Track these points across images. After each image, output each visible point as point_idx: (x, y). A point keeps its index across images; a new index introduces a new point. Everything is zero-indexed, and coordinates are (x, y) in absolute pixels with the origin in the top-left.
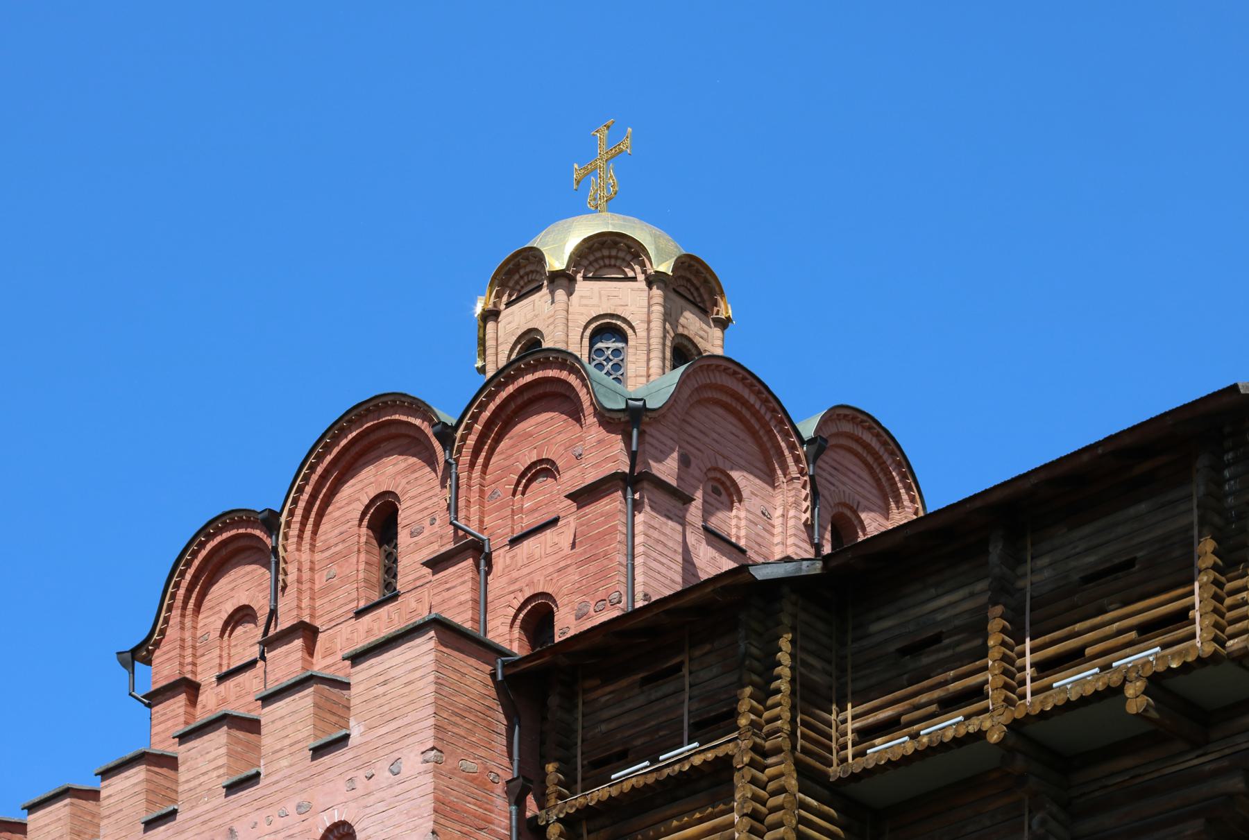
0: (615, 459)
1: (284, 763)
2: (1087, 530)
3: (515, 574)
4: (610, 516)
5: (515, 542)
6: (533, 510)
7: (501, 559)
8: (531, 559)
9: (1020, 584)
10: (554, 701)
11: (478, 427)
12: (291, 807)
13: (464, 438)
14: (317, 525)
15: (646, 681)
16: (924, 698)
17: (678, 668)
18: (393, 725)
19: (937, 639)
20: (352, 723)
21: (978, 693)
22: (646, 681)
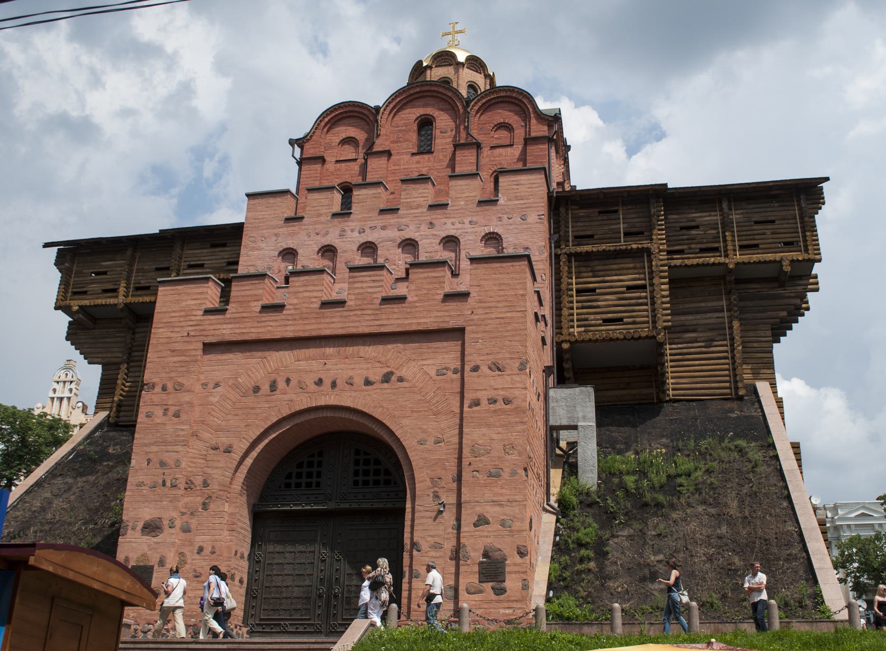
0: (544, 131)
1: (462, 203)
2: (751, 206)
3: (492, 159)
4: (542, 150)
5: (492, 148)
6: (497, 138)
7: (486, 151)
8: (500, 155)
9: (731, 217)
10: (562, 210)
11: (480, 104)
12: (467, 221)
13: (473, 106)
14: (393, 117)
15: (600, 213)
16: (693, 246)
17: (616, 211)
18: (522, 202)
19: (696, 227)
20: (500, 195)
21: (716, 249)
22: (600, 213)
